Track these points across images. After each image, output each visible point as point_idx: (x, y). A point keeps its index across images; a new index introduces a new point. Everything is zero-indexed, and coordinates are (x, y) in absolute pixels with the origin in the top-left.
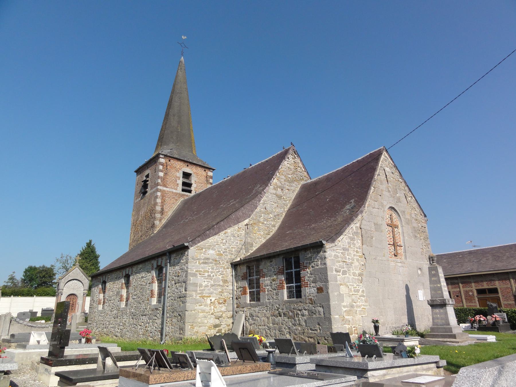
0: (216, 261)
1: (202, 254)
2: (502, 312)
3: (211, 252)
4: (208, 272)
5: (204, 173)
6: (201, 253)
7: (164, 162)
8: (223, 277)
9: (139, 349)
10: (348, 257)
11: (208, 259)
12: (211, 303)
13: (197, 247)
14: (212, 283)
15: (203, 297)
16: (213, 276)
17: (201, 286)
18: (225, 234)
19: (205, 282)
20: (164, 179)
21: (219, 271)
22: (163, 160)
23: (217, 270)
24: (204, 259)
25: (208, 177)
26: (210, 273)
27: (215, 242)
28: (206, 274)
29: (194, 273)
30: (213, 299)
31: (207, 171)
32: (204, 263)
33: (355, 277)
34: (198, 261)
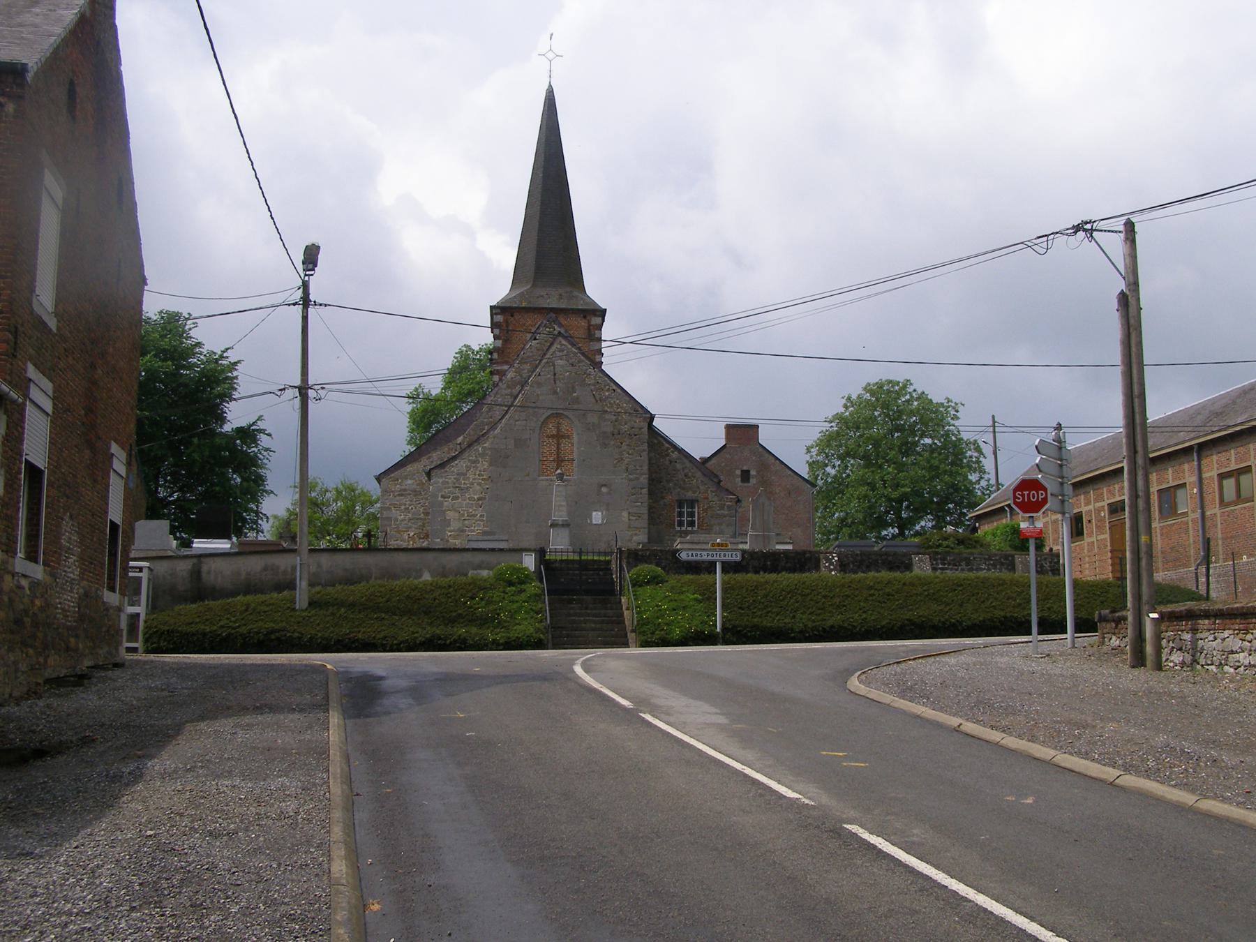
0: (416, 491)
1: (398, 486)
2: (1046, 550)
3: (409, 482)
4: (405, 504)
5: (584, 323)
6: (396, 485)
7: (502, 321)
8: (424, 509)
9: (114, 522)
10: (463, 482)
11: (405, 490)
12: (409, 537)
13: (391, 478)
14: (410, 515)
15: (399, 532)
16: (412, 508)
17: (396, 520)
18: (429, 458)
19: (401, 515)
20: (503, 351)
21: (420, 503)
22: (499, 316)
23: (417, 502)
24: (399, 491)
25: (591, 327)
26: (407, 506)
27: (414, 470)
28: (403, 507)
29: (388, 507)
30: (412, 534)
31: (588, 318)
32: (399, 495)
33: (471, 502)
34: (392, 494)
